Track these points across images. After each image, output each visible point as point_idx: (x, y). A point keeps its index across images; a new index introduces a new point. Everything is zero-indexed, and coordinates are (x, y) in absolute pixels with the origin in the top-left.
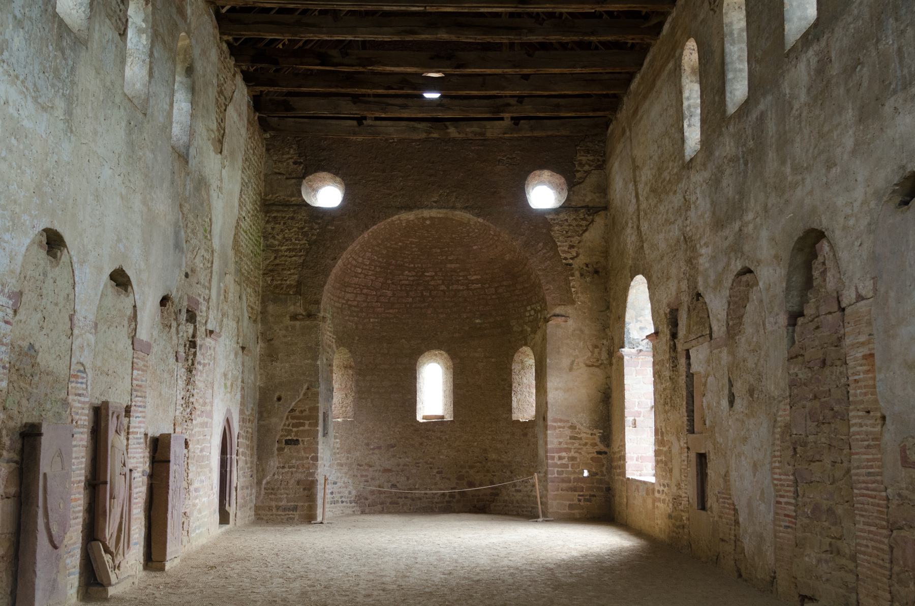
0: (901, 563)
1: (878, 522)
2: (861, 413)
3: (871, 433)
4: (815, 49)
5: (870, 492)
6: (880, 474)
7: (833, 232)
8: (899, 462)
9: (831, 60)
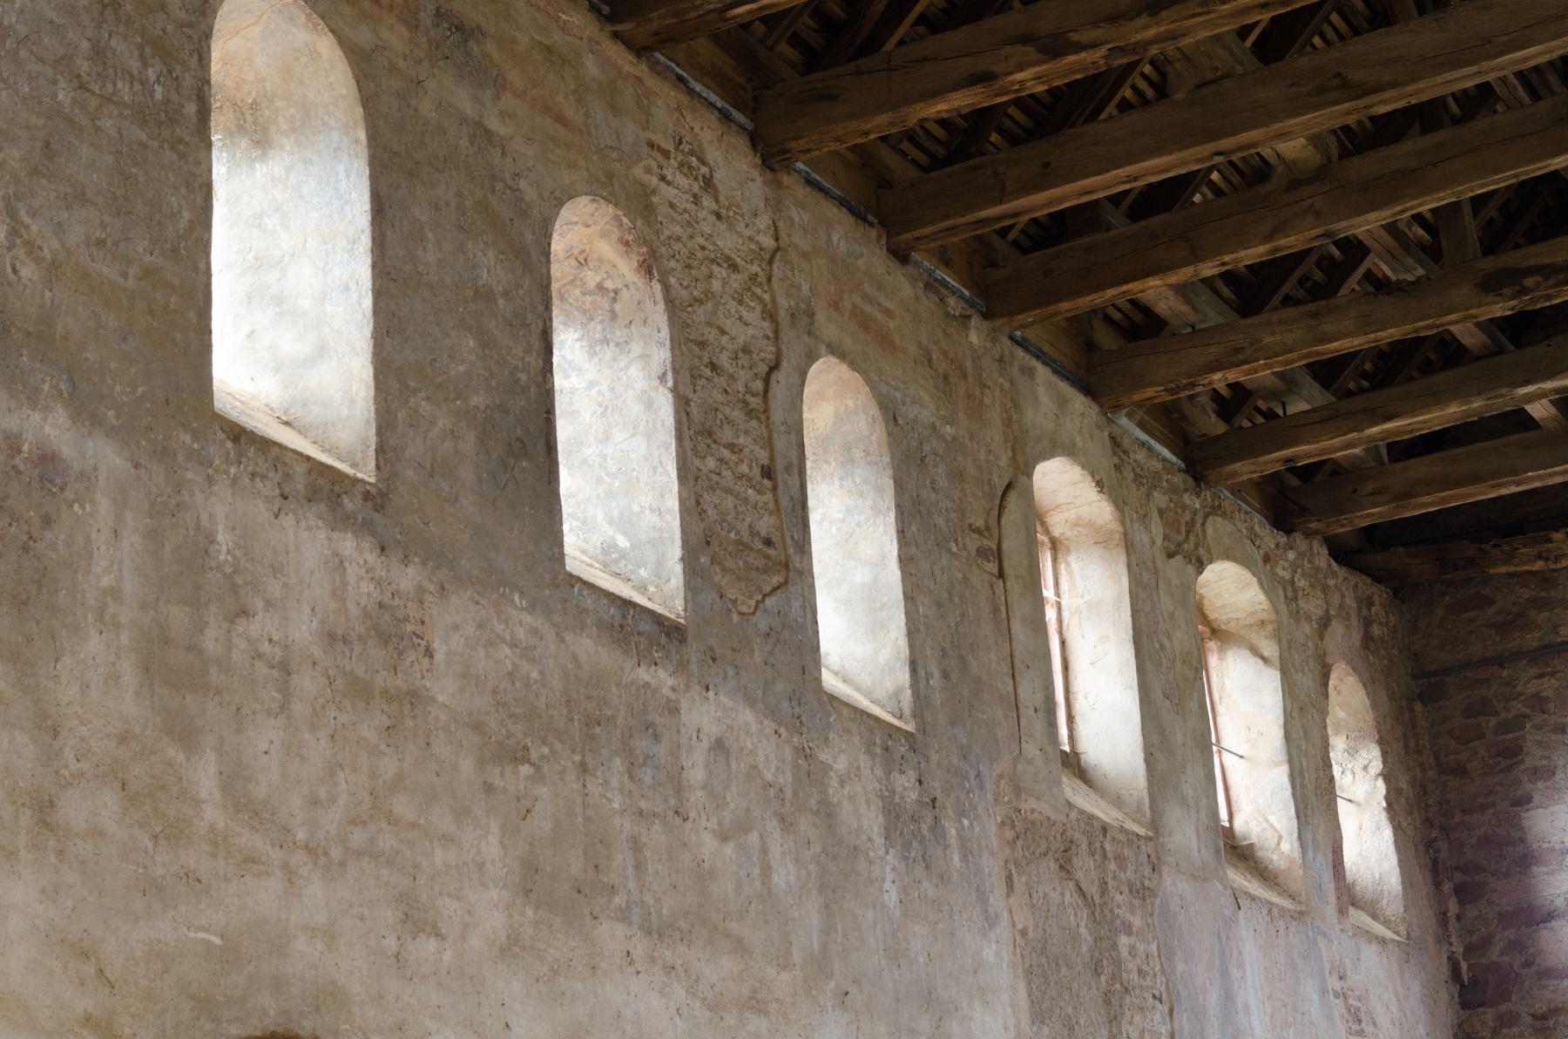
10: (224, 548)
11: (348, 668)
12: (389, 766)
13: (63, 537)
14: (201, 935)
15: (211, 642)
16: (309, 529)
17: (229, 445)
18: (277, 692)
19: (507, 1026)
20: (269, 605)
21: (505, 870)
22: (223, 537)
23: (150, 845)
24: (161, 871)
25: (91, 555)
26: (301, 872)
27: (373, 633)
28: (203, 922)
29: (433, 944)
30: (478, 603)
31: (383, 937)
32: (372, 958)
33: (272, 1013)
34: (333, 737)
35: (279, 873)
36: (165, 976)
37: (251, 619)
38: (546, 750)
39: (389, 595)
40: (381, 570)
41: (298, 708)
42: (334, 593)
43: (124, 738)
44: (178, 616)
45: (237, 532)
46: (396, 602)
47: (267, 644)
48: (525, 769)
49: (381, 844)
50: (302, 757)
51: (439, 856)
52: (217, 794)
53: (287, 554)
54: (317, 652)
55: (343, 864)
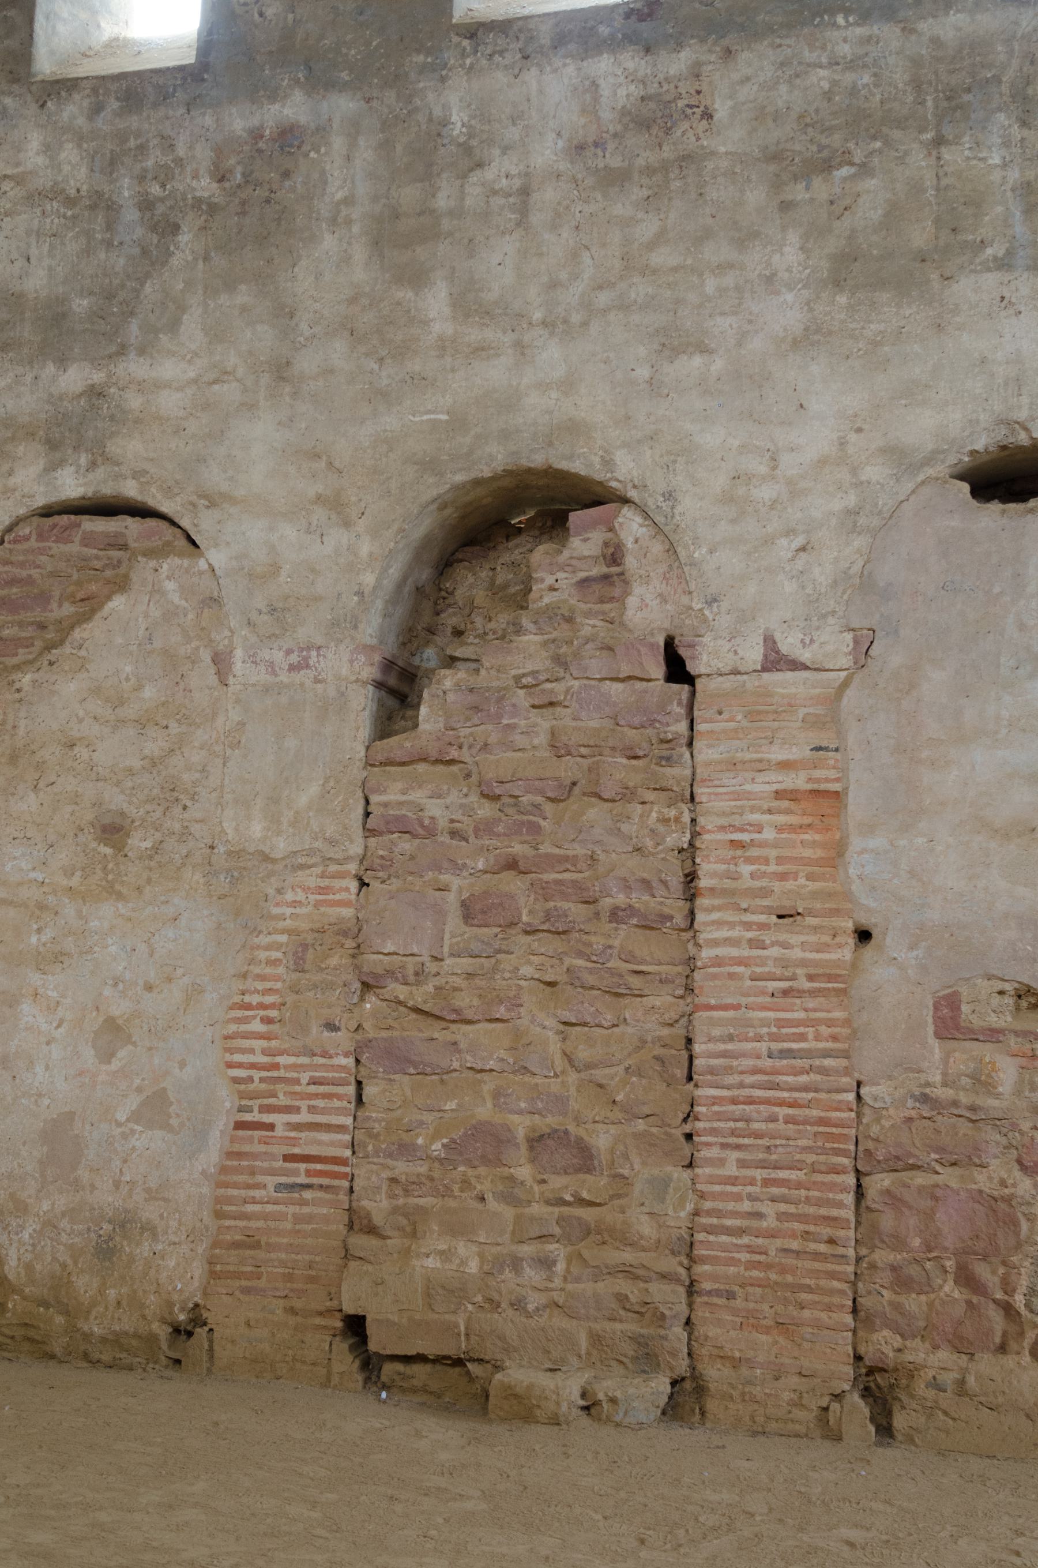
0: (917, 1242)
1: (810, 1158)
2: (762, 918)
3: (803, 963)
4: (630, 65)
5: (785, 1095)
6: (846, 1055)
7: (669, 496)
8: (931, 1029)
9: (708, 115)
10: (459, 124)
11: (601, 165)
12: (647, 228)
13: (300, 180)
14: (425, 417)
15: (443, 201)
16: (555, 71)
17: (466, 43)
18: (514, 213)
19: (801, 406)
20: (505, 150)
21: (808, 271)
22: (458, 118)
23: (376, 367)
24: (385, 382)
25: (326, 183)
26: (535, 343)
27: (631, 126)
28: (429, 407)
29: (698, 360)
30: (780, 46)
31: (633, 370)
32: (618, 390)
33: (500, 457)
34: (577, 228)
35: (510, 351)
36: (390, 454)
37: (486, 168)
38: (878, 144)
39: (656, 85)
40: (646, 68)
41: (536, 218)
42: (583, 111)
43: (353, 300)
44: (409, 195)
45: (473, 107)
46: (666, 87)
47: (504, 180)
48: (845, 171)
49: (633, 296)
50: (541, 254)
51: (711, 285)
52: (447, 311)
53: (529, 100)
54: (563, 166)
55: (585, 324)
